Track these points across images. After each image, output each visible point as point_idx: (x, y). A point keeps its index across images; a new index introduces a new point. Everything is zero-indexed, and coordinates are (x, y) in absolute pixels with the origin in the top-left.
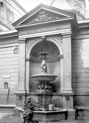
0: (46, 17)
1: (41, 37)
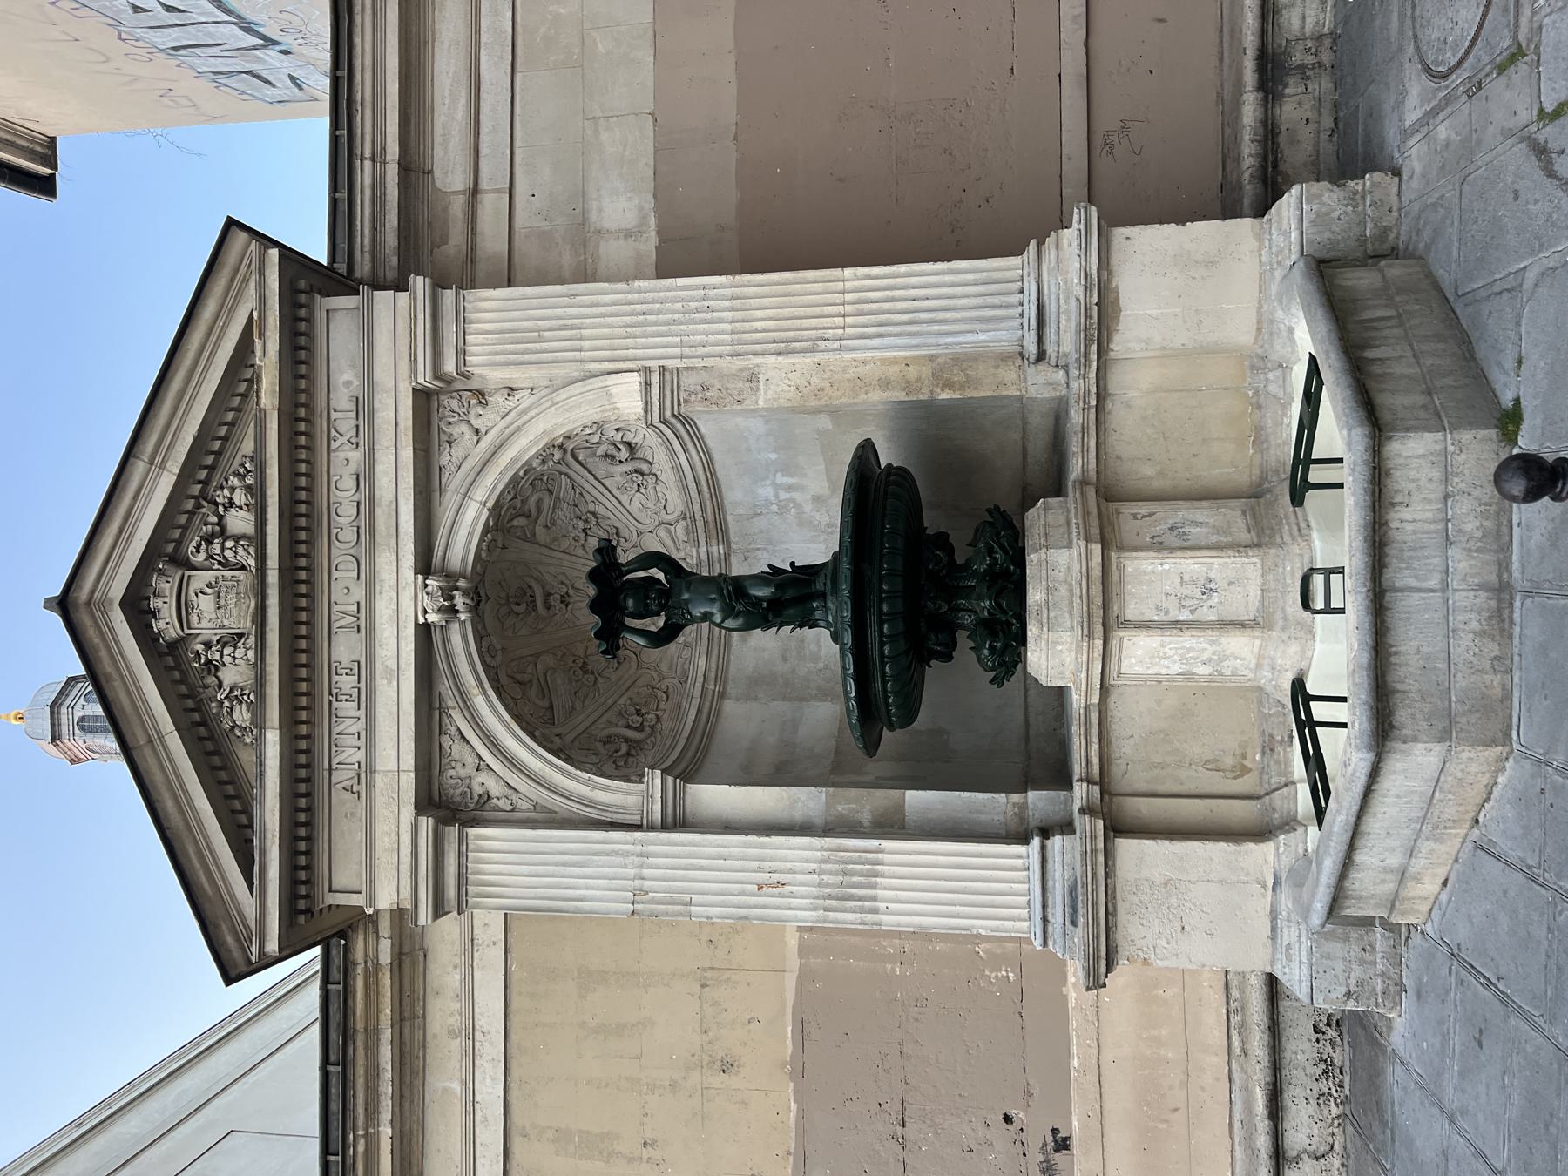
0: (225, 564)
1: (424, 632)
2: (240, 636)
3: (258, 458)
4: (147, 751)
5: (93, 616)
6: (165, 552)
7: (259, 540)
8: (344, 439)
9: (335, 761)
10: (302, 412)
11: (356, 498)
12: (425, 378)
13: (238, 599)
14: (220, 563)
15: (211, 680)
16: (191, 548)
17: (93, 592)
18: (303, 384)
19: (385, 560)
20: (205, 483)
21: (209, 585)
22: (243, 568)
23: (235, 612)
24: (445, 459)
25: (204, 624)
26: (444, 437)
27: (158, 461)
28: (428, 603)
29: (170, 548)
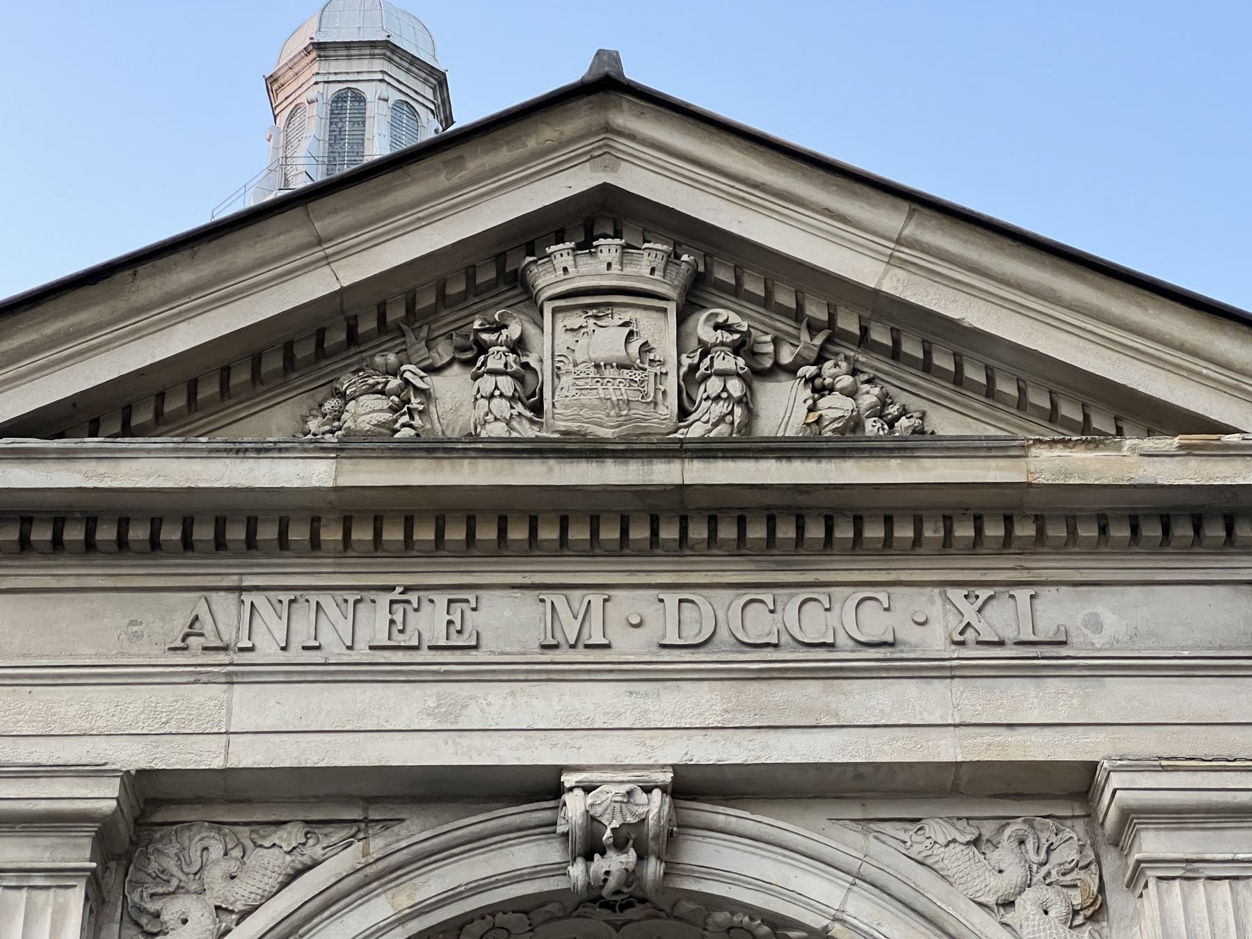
0: (691, 378)
1: (544, 786)
2: (538, 409)
3: (922, 443)
4: (300, 235)
5: (582, 137)
6: (710, 265)
7: (746, 445)
8: (970, 614)
9: (259, 599)
10: (1026, 530)
11: (842, 640)
12: (1121, 789)
13: (616, 405)
14: (694, 368)
15: (443, 352)
16: (723, 315)
17: (632, 137)
18: (1088, 532)
19: (705, 701)
20: (863, 340)
21: (645, 348)
22: (683, 413)
23: (587, 398)
24: (938, 830)
25: (564, 340)
26: (988, 829)
27: (906, 253)
28: (608, 794)
29: (724, 275)
